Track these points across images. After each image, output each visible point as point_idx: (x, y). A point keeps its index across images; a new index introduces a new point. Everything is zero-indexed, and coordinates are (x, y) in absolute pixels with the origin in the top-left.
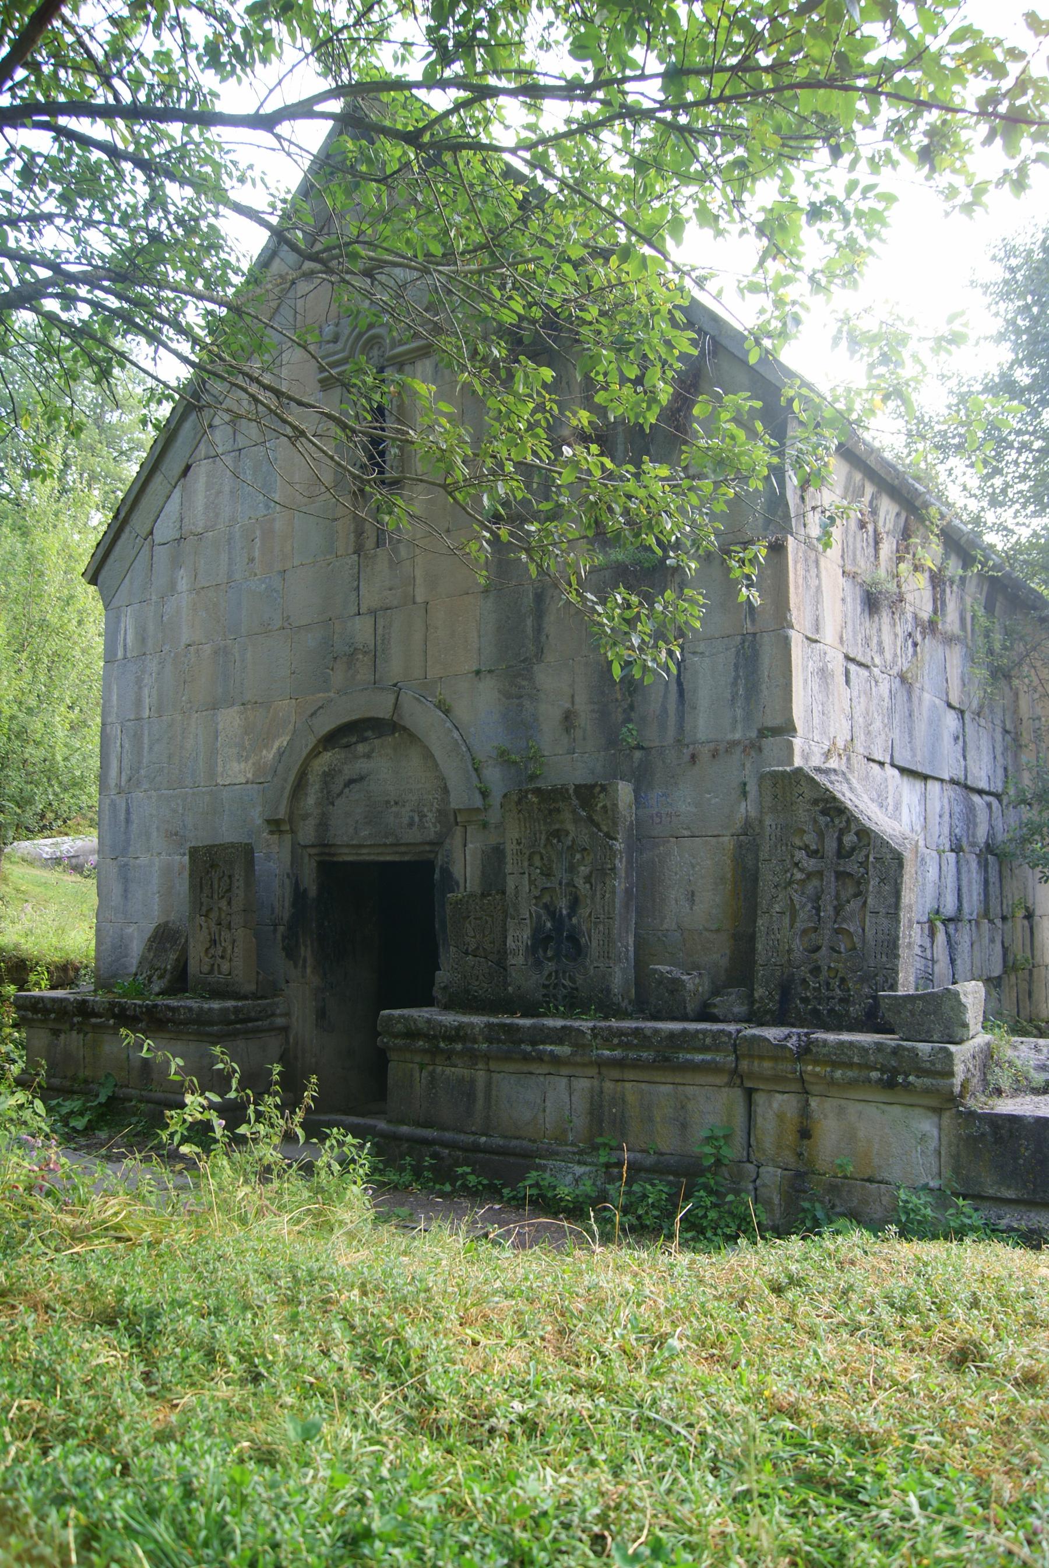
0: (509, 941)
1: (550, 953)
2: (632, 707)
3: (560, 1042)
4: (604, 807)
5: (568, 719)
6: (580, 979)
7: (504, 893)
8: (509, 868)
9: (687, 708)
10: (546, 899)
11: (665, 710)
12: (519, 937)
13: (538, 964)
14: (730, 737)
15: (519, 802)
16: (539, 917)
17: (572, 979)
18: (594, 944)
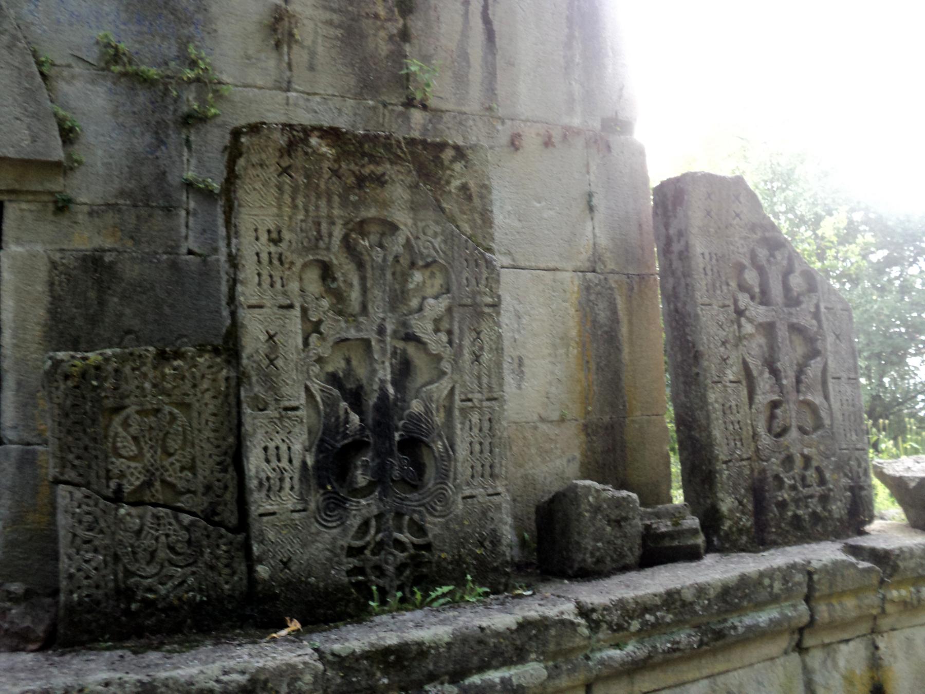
0: (255, 463)
1: (361, 479)
2: (405, 35)
3: (520, 656)
4: (464, 188)
5: (279, 29)
6: (434, 525)
7: (229, 347)
8: (247, 293)
9: (500, 63)
10: (337, 365)
11: (464, 56)
12: (278, 449)
13: (335, 505)
14: (566, 120)
15: (290, 148)
16: (330, 403)
17: (419, 529)
18: (462, 451)
